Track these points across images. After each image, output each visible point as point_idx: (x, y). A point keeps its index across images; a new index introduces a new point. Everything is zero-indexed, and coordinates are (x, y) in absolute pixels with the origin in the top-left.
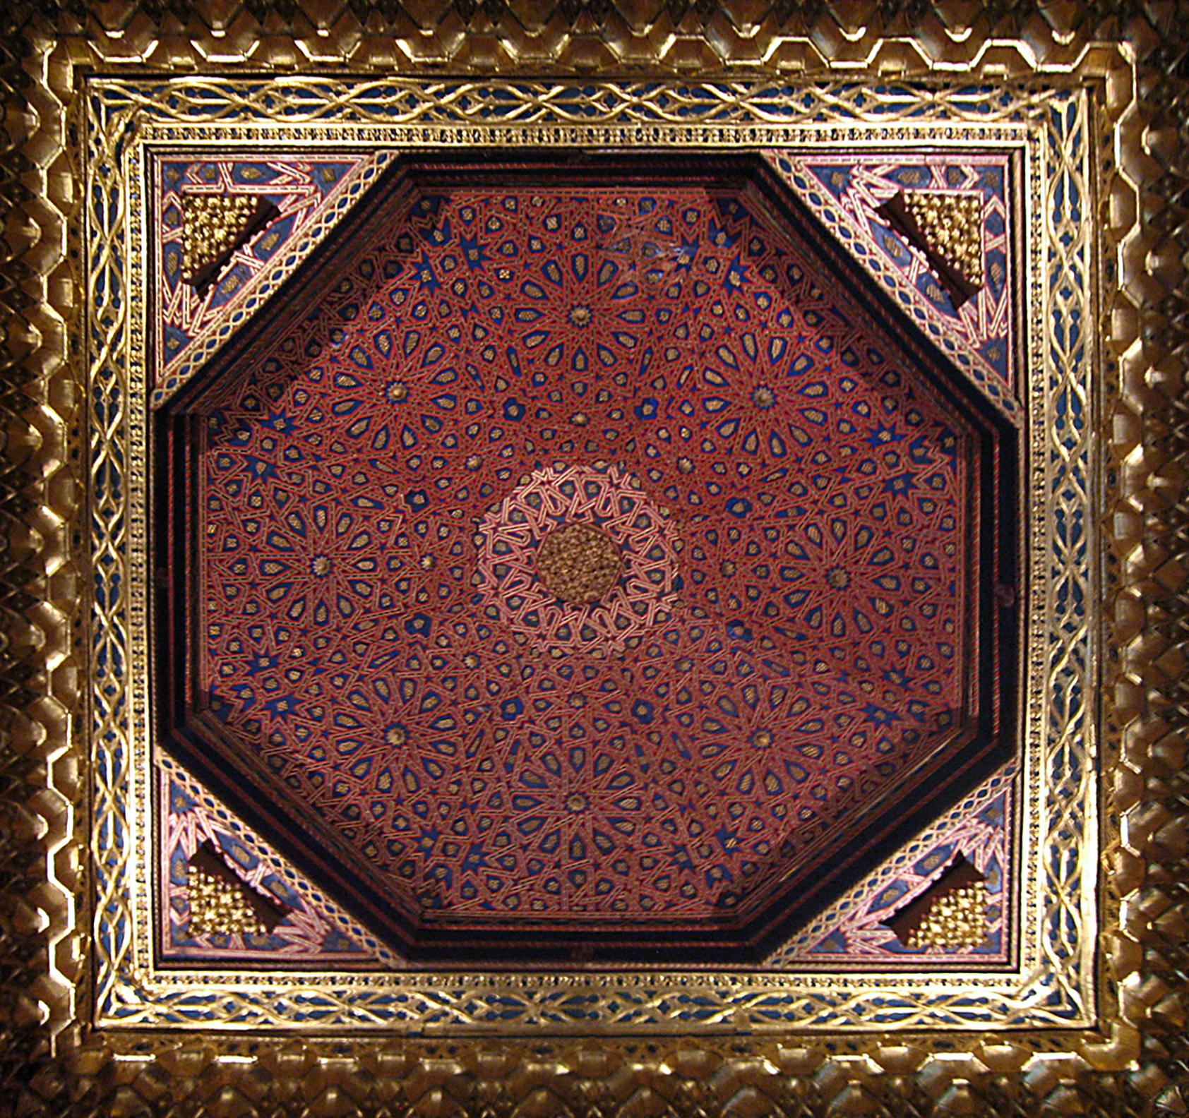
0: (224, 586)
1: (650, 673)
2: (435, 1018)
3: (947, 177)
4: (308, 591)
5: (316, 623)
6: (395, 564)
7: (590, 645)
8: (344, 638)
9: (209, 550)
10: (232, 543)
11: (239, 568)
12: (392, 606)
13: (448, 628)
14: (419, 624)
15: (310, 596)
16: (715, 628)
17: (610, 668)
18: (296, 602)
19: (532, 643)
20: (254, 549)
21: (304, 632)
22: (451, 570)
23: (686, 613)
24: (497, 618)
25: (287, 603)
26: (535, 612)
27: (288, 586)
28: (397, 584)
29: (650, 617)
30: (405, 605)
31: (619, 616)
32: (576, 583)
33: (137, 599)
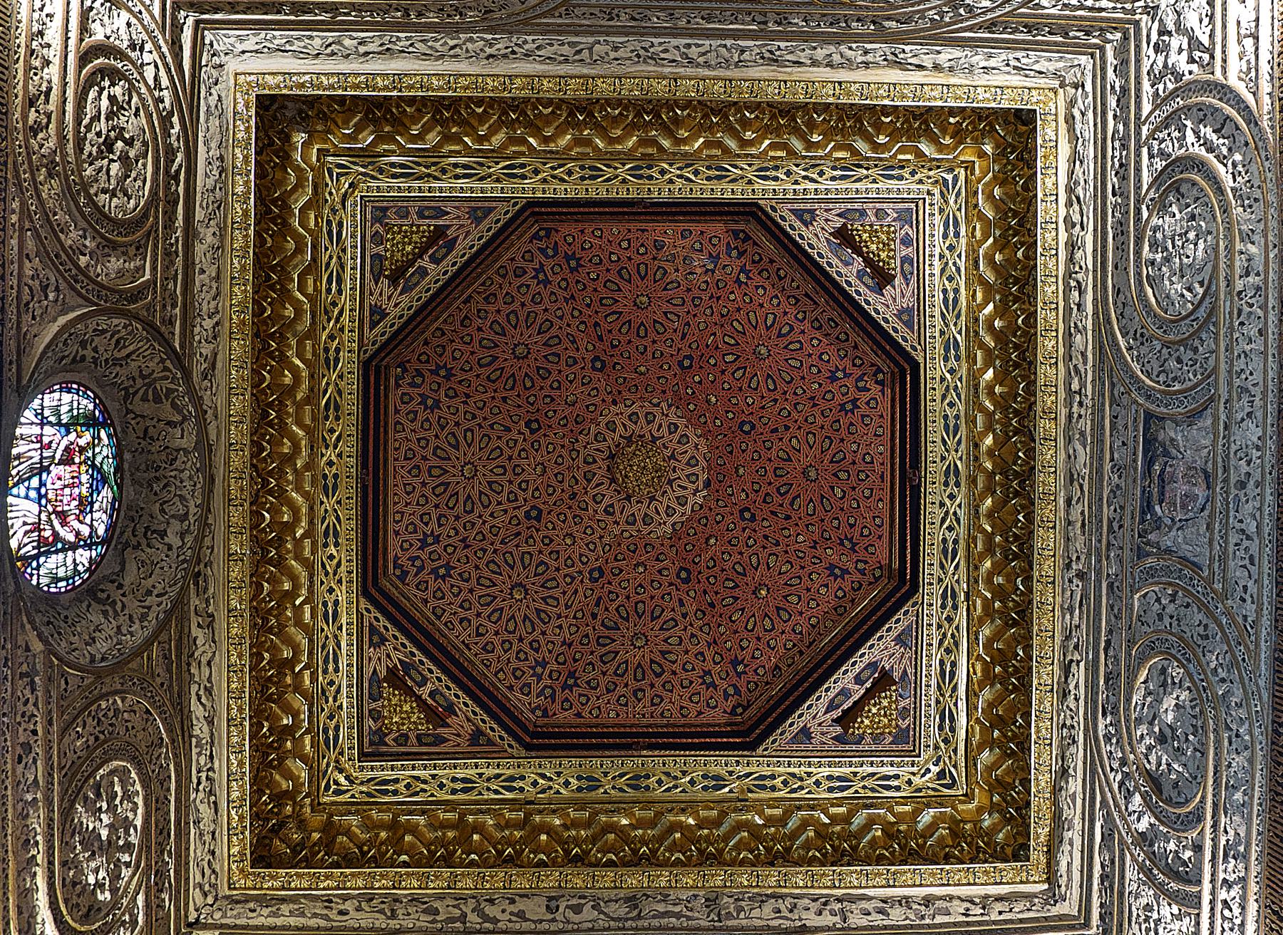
2: (543, 791)
6: (518, 470)
7: (649, 529)
8: (484, 522)
9: (396, 460)
11: (415, 472)
20: (425, 458)
26: (612, 506)
30: (525, 500)
31: (668, 507)
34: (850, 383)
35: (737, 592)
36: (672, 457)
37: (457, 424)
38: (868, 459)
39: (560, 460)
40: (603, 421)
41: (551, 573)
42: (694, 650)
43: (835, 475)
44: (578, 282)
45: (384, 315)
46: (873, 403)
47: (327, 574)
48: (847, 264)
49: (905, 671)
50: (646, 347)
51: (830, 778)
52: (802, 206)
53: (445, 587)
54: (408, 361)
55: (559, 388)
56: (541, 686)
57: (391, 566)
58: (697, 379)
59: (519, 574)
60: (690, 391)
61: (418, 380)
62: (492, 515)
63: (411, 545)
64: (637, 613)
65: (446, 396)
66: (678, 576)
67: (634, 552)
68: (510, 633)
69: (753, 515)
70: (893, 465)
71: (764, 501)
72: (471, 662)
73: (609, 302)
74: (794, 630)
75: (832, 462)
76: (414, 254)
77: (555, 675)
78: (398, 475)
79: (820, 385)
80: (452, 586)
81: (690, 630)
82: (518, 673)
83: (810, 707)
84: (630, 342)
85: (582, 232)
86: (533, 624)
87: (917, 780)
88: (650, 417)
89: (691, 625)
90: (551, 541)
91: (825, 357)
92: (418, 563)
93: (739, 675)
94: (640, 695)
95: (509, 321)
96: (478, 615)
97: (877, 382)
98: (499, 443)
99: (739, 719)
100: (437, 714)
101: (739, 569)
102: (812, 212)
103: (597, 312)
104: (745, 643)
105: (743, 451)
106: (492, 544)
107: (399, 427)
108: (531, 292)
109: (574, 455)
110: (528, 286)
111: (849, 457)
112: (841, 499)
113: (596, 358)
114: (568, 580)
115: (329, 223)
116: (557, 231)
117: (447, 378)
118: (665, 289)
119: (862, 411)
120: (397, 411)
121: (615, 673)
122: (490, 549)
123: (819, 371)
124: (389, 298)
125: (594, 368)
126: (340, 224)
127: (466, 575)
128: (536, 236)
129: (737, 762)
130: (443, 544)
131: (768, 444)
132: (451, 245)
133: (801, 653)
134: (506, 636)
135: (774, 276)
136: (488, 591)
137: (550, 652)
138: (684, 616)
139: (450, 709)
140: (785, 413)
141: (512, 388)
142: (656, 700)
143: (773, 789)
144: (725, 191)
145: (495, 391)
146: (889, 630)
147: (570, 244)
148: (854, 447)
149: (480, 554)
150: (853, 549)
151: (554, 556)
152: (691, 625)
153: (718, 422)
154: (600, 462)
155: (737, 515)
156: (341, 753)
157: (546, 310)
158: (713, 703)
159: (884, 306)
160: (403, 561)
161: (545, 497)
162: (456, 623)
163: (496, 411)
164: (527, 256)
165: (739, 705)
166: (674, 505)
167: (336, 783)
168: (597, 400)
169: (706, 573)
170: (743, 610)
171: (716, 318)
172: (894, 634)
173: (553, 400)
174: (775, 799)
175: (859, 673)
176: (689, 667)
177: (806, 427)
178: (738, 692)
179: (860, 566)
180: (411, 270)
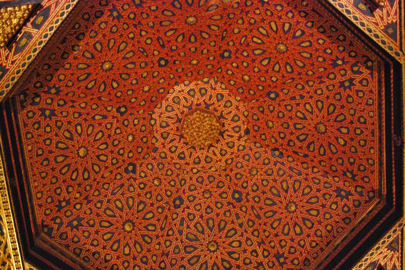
1: (238, 176)
6: (116, 143)
8: (98, 183)
9: (31, 158)
10: (40, 152)
11: (45, 163)
12: (118, 162)
13: (144, 168)
14: (131, 168)
15: (80, 167)
16: (266, 152)
17: (220, 175)
20: (51, 152)
21: (79, 185)
22: (142, 140)
24: (166, 158)
26: (183, 153)
27: (69, 165)
28: (118, 152)
30: (123, 161)
31: (221, 150)
32: (201, 139)
34: (347, 67)
35: (275, 208)
36: (222, 116)
37: (69, 123)
38: (362, 120)
39: (143, 128)
41: (148, 208)
42: (250, 249)
43: (338, 130)
44: (142, 13)
46: (364, 83)
49: (394, 266)
54: (28, 89)
58: (234, 65)
60: (230, 72)
61: (38, 100)
63: (51, 211)
64: (209, 228)
65: (59, 105)
67: (202, 183)
69: (281, 154)
71: (288, 145)
73: (167, 23)
74: (315, 234)
75: (335, 121)
76: (18, 24)
79: (325, 69)
84: (184, 47)
86: (141, 246)
89: (246, 231)
90: (145, 185)
92: (58, 221)
96: (104, 248)
97: (367, 68)
101: (274, 191)
103: (158, 31)
104: (283, 243)
105: (271, 112)
106: (106, 196)
107: (29, 136)
109: (153, 122)
111: (349, 118)
112: (344, 146)
114: (160, 210)
118: (207, 10)
119: (356, 88)
120: (25, 125)
123: (325, 60)
124: (7, 58)
127: (92, 222)
130: (72, 205)
131: (289, 108)
132: (46, 14)
133: (322, 249)
136: (108, 230)
137: (155, 262)
138: (241, 225)
140: (300, 87)
141: (104, 90)
145: (93, 94)
146: (384, 242)
148: (352, 112)
149: (99, 205)
150: (353, 178)
151: (148, 196)
152: (246, 231)
153: (252, 92)
163: (94, 106)
169: (252, 194)
172: (387, 244)
176: (247, 261)
180: (19, 36)
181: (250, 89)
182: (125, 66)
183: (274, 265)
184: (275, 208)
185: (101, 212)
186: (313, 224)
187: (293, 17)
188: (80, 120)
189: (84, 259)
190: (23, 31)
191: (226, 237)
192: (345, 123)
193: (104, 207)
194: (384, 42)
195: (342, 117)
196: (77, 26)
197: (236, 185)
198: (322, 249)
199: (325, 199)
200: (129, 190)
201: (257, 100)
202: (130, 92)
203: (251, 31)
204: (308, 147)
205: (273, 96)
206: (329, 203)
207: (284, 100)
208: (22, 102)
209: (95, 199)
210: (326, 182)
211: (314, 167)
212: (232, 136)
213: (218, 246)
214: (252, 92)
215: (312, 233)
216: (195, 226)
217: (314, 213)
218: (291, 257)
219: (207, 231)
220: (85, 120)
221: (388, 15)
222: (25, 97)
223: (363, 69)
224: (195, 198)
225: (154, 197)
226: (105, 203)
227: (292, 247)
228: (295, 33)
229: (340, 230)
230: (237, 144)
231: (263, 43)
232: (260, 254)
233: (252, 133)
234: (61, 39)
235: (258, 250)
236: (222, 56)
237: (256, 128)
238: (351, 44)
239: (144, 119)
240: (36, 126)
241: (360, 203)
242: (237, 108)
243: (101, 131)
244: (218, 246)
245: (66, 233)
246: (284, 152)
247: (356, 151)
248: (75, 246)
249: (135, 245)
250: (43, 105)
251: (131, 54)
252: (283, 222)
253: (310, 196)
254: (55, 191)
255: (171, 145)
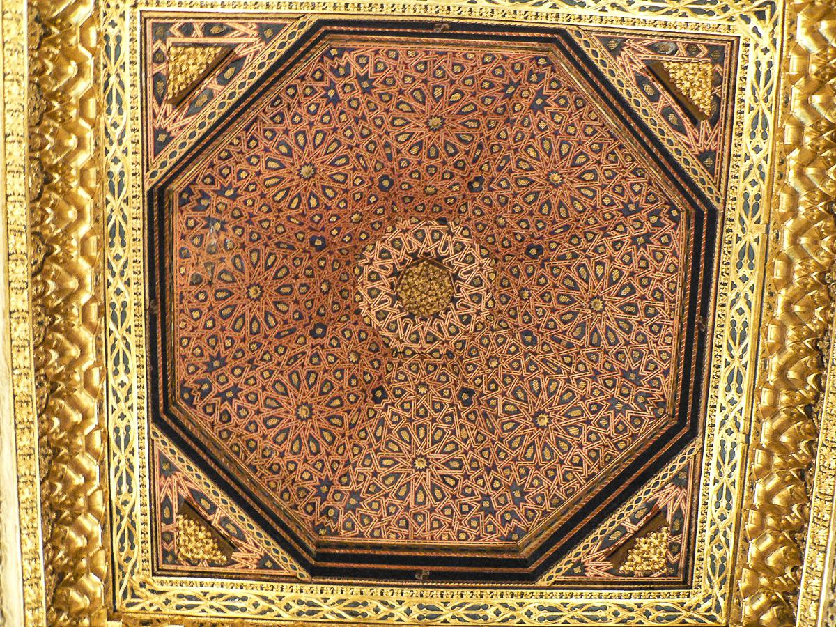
0: (432, 529)
1: (506, 243)
3: (159, 63)
4: (437, 473)
5: (460, 468)
6: (422, 412)
7: (486, 282)
8: (472, 449)
9: (407, 537)
10: (403, 523)
11: (420, 519)
14: (465, 397)
15: (441, 472)
16: (474, 199)
17: (503, 269)
18: (445, 482)
19: (482, 320)
20: (407, 508)
23: (464, 217)
24: (464, 342)
25: (446, 489)
26: (461, 317)
29: (465, 240)
30: (452, 405)
33: (434, 597)
34: (339, 82)
37: (375, 474)
38: (421, 67)
39: (414, 367)
40: (375, 322)
42: (610, 251)
45: (266, 557)
46: (362, 61)
47: (513, 617)
48: (211, 96)
50: (302, 285)
51: (753, 136)
52: (151, 143)
53: (533, 492)
54: (313, 523)
55: (342, 371)
56: (634, 406)
57: (511, 544)
58: (335, 232)
59: (524, 419)
60: (347, 239)
61: (331, 512)
62: (465, 441)
63: (490, 523)
64: (570, 303)
65: (347, 484)
66: (534, 257)
67: (508, 298)
68: (581, 432)
69: (477, 179)
70: (428, 43)
71: (463, 168)
72: (607, 474)
74: (597, 152)
75: (423, 103)
76: (208, 530)
77: (625, 391)
78: (421, 535)
79: (342, 112)
80: (531, 486)
81: (590, 253)
82: (620, 427)
83: (678, 152)
84: (296, 302)
85: (184, 357)
86: (573, 409)
87: (765, 42)
88: (374, 277)
89: (584, 251)
90: (493, 381)
91: (313, 108)
92: (508, 517)
93: (639, 210)
94: (651, 311)
95: (274, 426)
96: (561, 462)
97: (340, 56)
98: (395, 432)
99: (683, 214)
100: (655, 519)
101: (530, 198)
102: (157, 132)
103: (266, 336)
104: (607, 201)
106: (493, 442)
107: (376, 533)
108: (245, 404)
109: (409, 352)
110: (239, 408)
112: (463, 95)
113: (313, 333)
114: (532, 368)
115: (178, 607)
116: (184, 382)
117: (329, 484)
118: (242, 270)
119: (371, 71)
120: (361, 535)
121: (628, 332)
122: (498, 444)
123: (328, 114)
124: (250, 552)
125: (323, 335)
126: (180, 596)
128: (190, 402)
129: (728, 231)
132: (197, 495)
134: (583, 438)
135: (227, 162)
136: (539, 450)
137: (602, 393)
138: (575, 256)
139: (650, 505)
140: (371, 147)
141: (341, 418)
142: (658, 295)
143: (758, 197)
144: (135, 229)
145: (343, 436)
147: (197, 368)
148: (408, 80)
149: (502, 455)
151: (508, 380)
152: (584, 251)
153: (380, 211)
154: (418, 327)
155: (475, 195)
156: (682, 604)
157: (264, 388)
158: (664, 239)
159: (258, 56)
160: (505, 531)
161: (450, 384)
162: (568, 485)
164: (209, 410)
165: (669, 213)
166: (462, 255)
167: (709, 610)
168: (355, 329)
169: (533, 230)
170: (573, 199)
171: (271, 216)
173: (353, 376)
174: (770, 196)
175: (648, 96)
176: (627, 258)
177: (387, 126)
178: (656, 213)
179: (534, 78)
180: (223, 531)
181: (375, 213)
182: (310, 387)
183: (638, 220)
184: (555, 203)
185: (512, 454)
186: (582, 153)
187: (258, 157)
188: (374, 459)
189: (568, 496)
190: (217, 526)
191: (587, 282)
192: (426, 90)
193: (507, 449)
194: (282, 45)
195: (417, 94)
196: (236, 448)
197: (518, 249)
198: (621, 147)
199: (546, 128)
200: (493, 407)
201: (394, 203)
202: (354, 382)
203: (280, 210)
204: (466, 142)
205: (386, 183)
206: (553, 124)
207: (392, 169)
208: (329, 533)
209: (493, 458)
210: (522, 123)
211: (498, 137)
212: (446, 244)
213: (597, 297)
214: (380, 211)
215: (596, 156)
216: (565, 323)
217: (565, 148)
218: (629, 193)
219: (574, 307)
220: (377, 451)
221: (245, 35)
222: (323, 528)
223: (343, 62)
224: (526, 313)
225: (512, 372)
226: (502, 446)
227: (614, 189)
228: (283, 154)
229: (593, 116)
230: (458, 238)
231: (299, 195)
232: (620, 237)
233: (444, 215)
234: (248, 471)
235: (614, 238)
236: (319, 249)
237: (436, 209)
238: (302, 78)
239: (400, 364)
240: (366, 521)
241: (554, 80)
242: (404, 231)
243: (399, 432)
244: (597, 297)
245: (526, 510)
246: (473, 175)
247: (472, 78)
248: (547, 503)
249: (570, 417)
250: (340, 506)
251: (294, 377)
252: (576, 194)
253: (540, 150)
254: (463, 513)
255: (446, 332)
